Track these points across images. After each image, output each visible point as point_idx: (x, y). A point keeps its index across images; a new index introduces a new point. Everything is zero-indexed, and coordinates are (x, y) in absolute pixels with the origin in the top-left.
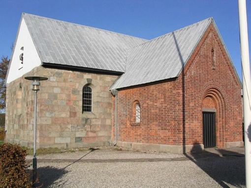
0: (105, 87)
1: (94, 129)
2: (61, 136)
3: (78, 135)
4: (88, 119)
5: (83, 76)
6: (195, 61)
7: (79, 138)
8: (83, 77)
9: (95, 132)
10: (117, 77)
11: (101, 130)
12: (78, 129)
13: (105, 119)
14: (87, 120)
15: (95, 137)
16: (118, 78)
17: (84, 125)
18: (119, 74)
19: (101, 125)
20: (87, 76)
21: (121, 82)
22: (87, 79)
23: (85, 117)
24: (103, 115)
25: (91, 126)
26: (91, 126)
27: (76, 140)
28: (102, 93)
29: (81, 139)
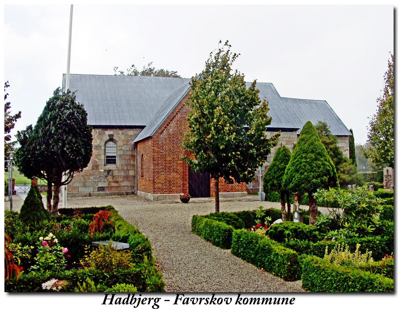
0: (128, 141)
1: (117, 180)
2: (85, 186)
3: (100, 185)
4: (110, 170)
5: (105, 133)
6: (177, 118)
7: (102, 187)
8: (104, 134)
9: (117, 182)
10: (141, 129)
11: (123, 180)
12: (101, 180)
13: (128, 170)
14: (109, 171)
15: (118, 187)
16: (142, 130)
17: (106, 176)
18: (142, 127)
19: (123, 176)
20: (109, 132)
21: (143, 135)
22: (109, 135)
23: (107, 169)
24: (126, 166)
25: (113, 177)
26: (113, 177)
27: (98, 189)
28: (125, 146)
29: (104, 189)
